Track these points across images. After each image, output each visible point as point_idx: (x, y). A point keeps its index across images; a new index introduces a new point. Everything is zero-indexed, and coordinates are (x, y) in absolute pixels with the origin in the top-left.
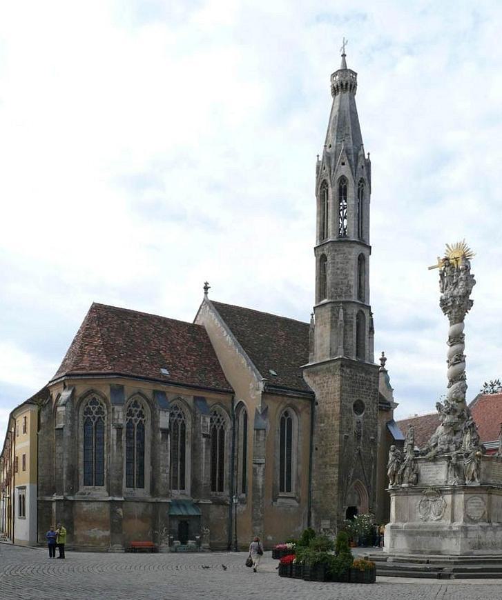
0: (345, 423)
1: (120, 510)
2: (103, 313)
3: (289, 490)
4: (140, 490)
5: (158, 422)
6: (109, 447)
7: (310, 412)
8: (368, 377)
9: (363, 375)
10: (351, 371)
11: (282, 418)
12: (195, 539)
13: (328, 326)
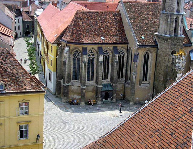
1: (84, 91)
2: (81, 15)
3: (146, 80)
4: (92, 81)
5: (99, 59)
6: (81, 68)
7: (156, 52)
8: (179, 41)
9: (177, 41)
10: (171, 40)
11: (145, 55)
12: (111, 98)
13: (164, 22)
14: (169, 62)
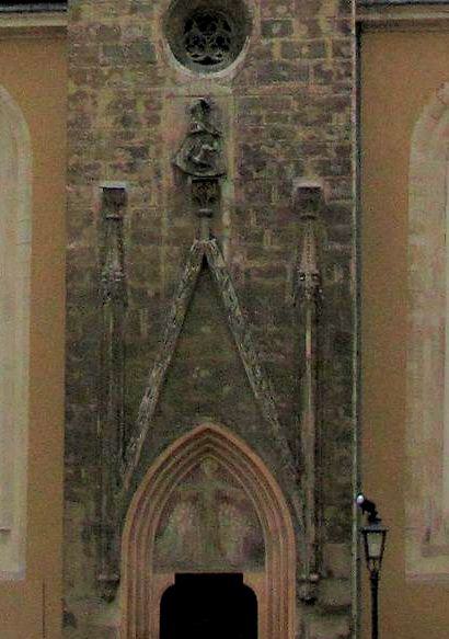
0: (103, 123)
14: (139, 153)
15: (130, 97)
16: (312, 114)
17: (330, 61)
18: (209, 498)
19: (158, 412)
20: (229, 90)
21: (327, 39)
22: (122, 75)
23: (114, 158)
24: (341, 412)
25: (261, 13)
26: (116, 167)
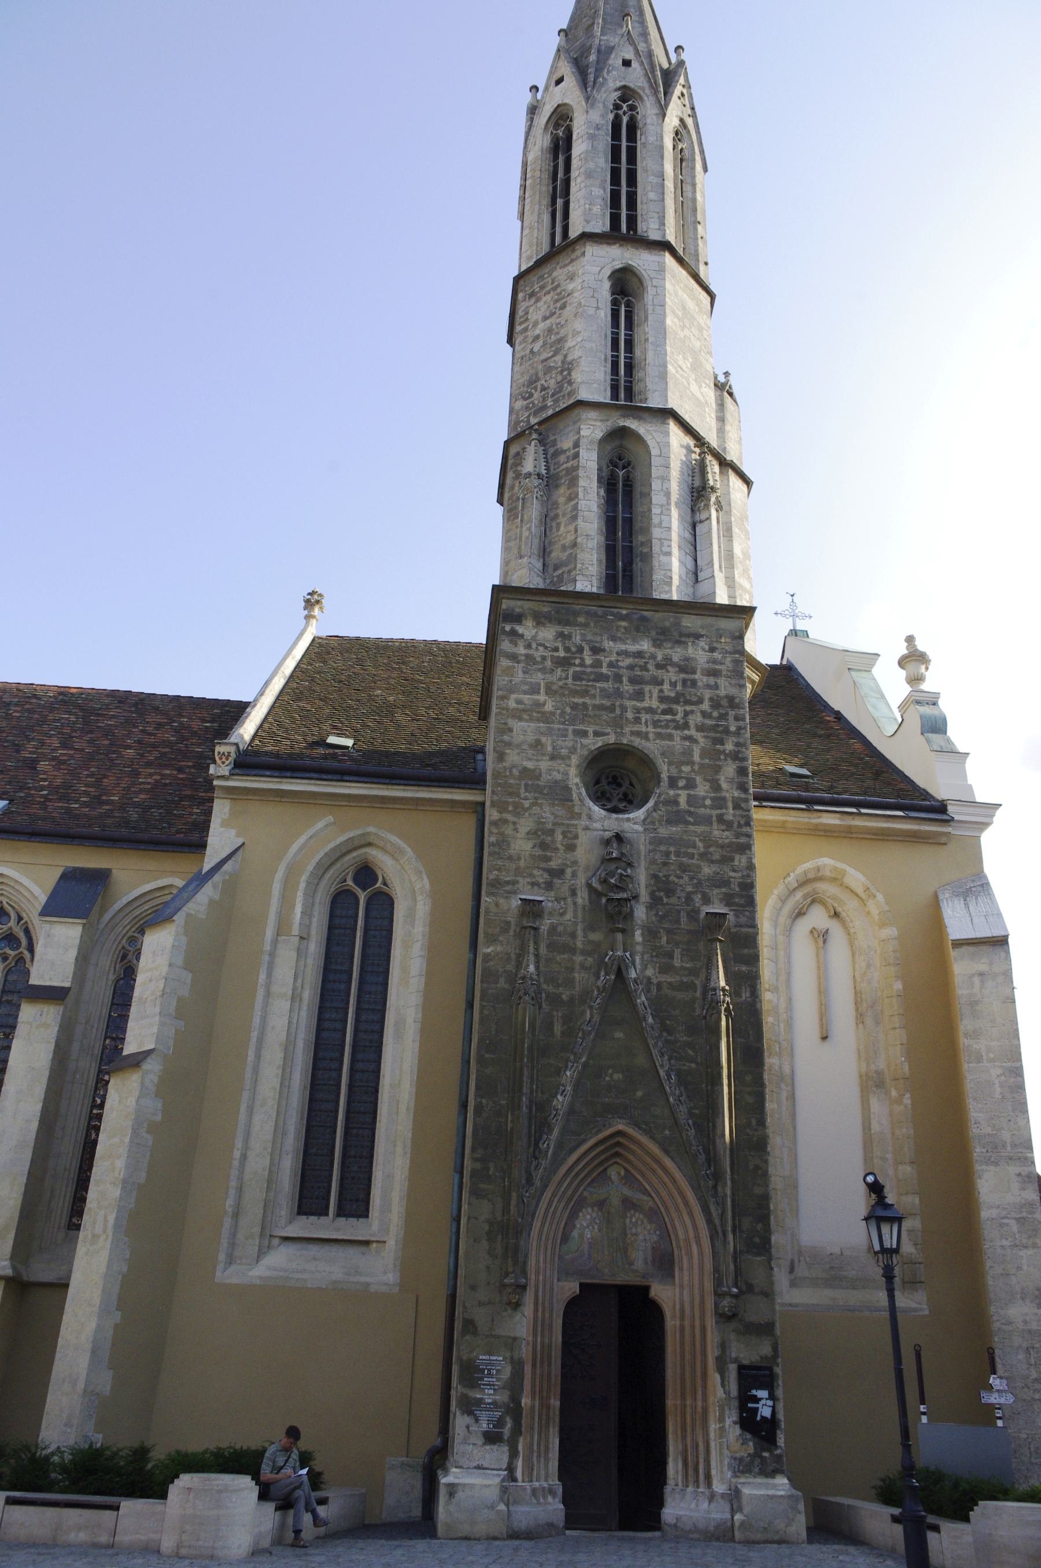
9: (645, 646)
14: (559, 873)
15: (549, 826)
16: (717, 854)
17: (730, 813)
18: (615, 1201)
19: (571, 1111)
20: (639, 828)
21: (727, 795)
22: (542, 809)
23: (531, 875)
24: (754, 1122)
25: (669, 770)
26: (533, 884)
